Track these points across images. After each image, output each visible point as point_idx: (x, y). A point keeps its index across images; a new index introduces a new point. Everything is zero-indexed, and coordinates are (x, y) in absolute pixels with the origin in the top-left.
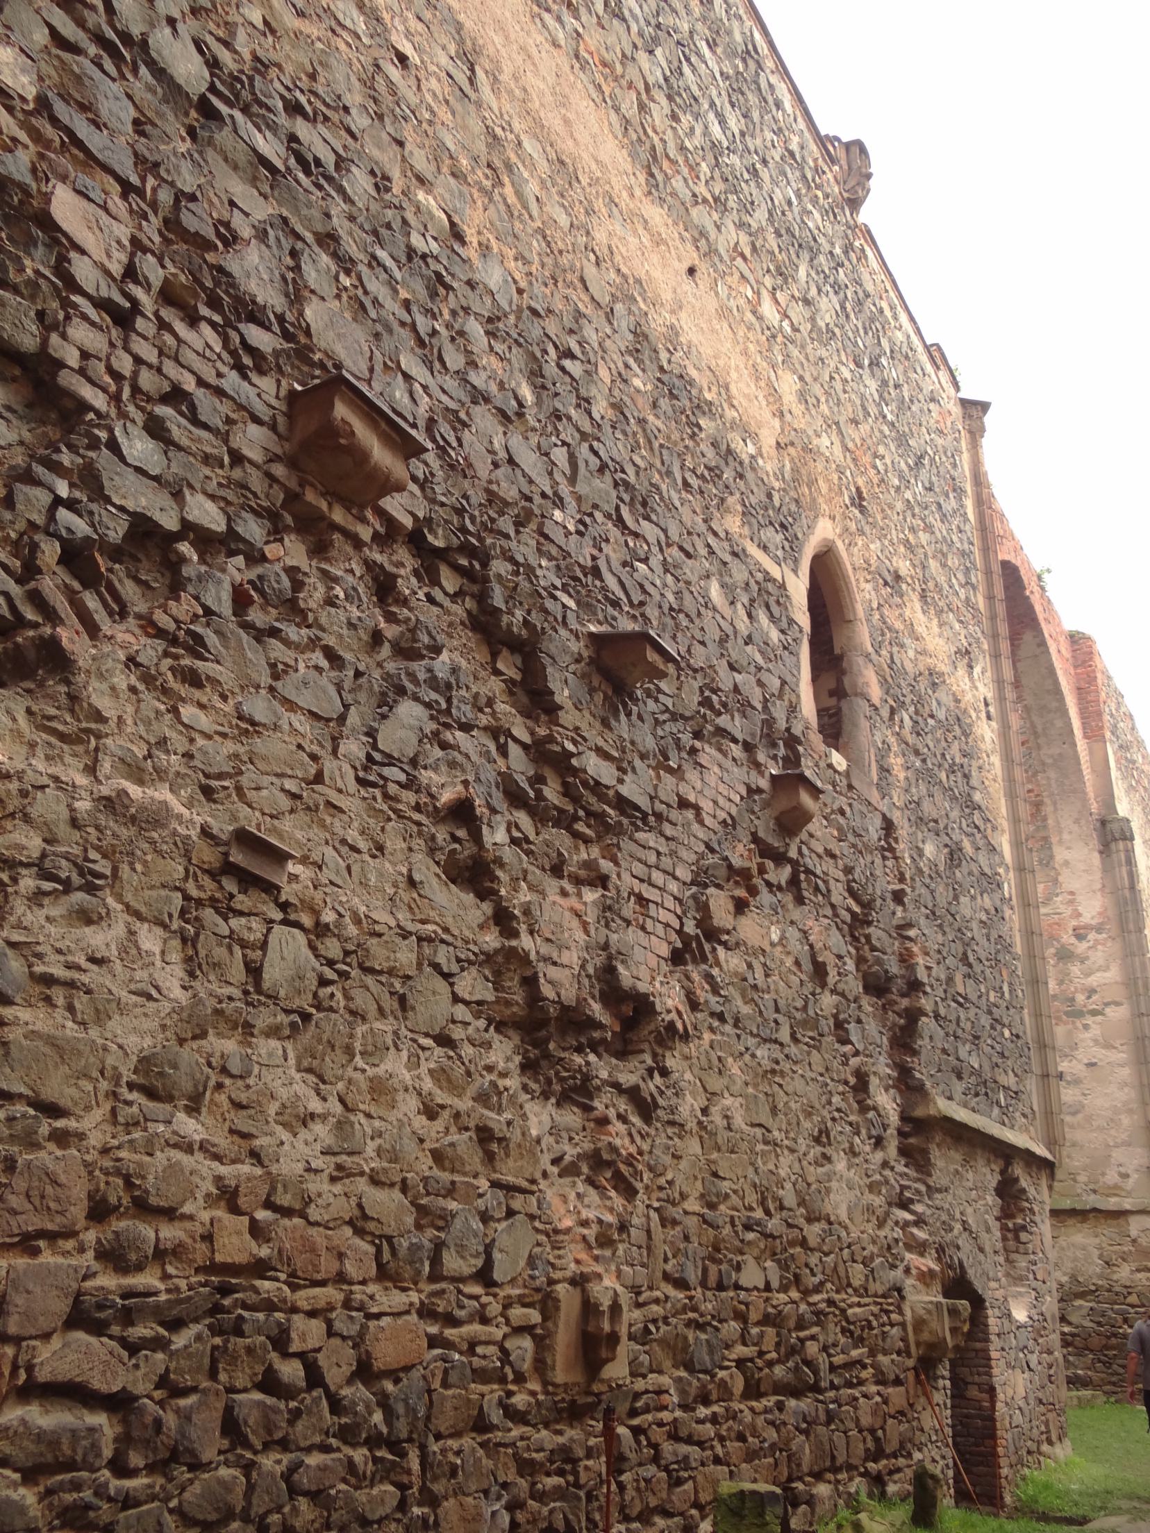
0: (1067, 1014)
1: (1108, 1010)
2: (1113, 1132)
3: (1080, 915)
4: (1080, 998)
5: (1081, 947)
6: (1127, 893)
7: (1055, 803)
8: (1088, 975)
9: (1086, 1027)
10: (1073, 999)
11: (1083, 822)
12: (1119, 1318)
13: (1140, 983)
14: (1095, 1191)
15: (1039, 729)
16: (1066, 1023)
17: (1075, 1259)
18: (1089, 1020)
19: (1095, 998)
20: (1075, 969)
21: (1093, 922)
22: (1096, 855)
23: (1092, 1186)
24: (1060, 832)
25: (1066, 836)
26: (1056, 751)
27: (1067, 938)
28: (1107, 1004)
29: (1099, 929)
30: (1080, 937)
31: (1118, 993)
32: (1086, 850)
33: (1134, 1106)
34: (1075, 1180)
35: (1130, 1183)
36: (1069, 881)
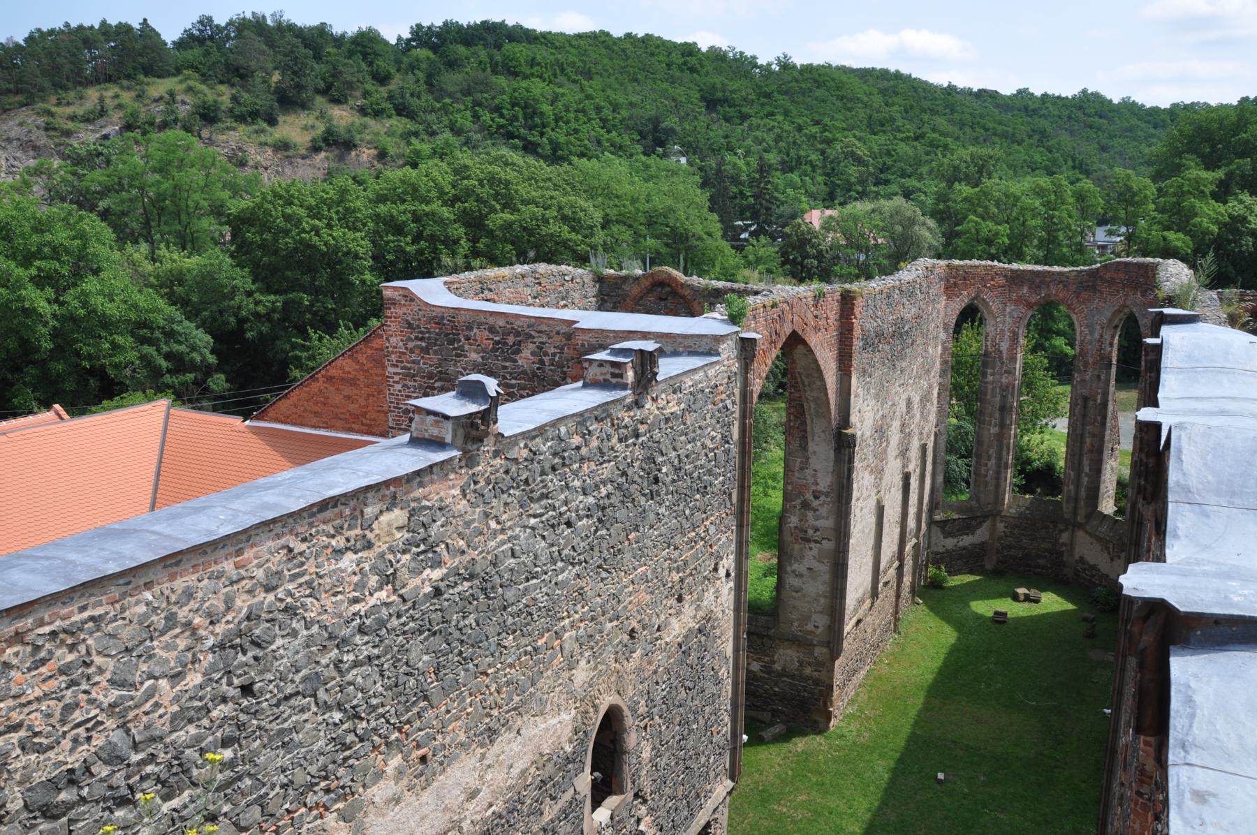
0: (802, 538)
1: (824, 542)
3: (818, 484)
4: (810, 532)
5: (815, 503)
6: (845, 481)
9: (811, 548)
10: (806, 532)
15: (806, 383)
17: (786, 661)
18: (813, 545)
19: (818, 533)
20: (810, 514)
22: (832, 452)
24: (813, 436)
25: (816, 438)
26: (815, 394)
27: (809, 496)
28: (824, 539)
29: (827, 495)
30: (816, 497)
35: (819, 632)
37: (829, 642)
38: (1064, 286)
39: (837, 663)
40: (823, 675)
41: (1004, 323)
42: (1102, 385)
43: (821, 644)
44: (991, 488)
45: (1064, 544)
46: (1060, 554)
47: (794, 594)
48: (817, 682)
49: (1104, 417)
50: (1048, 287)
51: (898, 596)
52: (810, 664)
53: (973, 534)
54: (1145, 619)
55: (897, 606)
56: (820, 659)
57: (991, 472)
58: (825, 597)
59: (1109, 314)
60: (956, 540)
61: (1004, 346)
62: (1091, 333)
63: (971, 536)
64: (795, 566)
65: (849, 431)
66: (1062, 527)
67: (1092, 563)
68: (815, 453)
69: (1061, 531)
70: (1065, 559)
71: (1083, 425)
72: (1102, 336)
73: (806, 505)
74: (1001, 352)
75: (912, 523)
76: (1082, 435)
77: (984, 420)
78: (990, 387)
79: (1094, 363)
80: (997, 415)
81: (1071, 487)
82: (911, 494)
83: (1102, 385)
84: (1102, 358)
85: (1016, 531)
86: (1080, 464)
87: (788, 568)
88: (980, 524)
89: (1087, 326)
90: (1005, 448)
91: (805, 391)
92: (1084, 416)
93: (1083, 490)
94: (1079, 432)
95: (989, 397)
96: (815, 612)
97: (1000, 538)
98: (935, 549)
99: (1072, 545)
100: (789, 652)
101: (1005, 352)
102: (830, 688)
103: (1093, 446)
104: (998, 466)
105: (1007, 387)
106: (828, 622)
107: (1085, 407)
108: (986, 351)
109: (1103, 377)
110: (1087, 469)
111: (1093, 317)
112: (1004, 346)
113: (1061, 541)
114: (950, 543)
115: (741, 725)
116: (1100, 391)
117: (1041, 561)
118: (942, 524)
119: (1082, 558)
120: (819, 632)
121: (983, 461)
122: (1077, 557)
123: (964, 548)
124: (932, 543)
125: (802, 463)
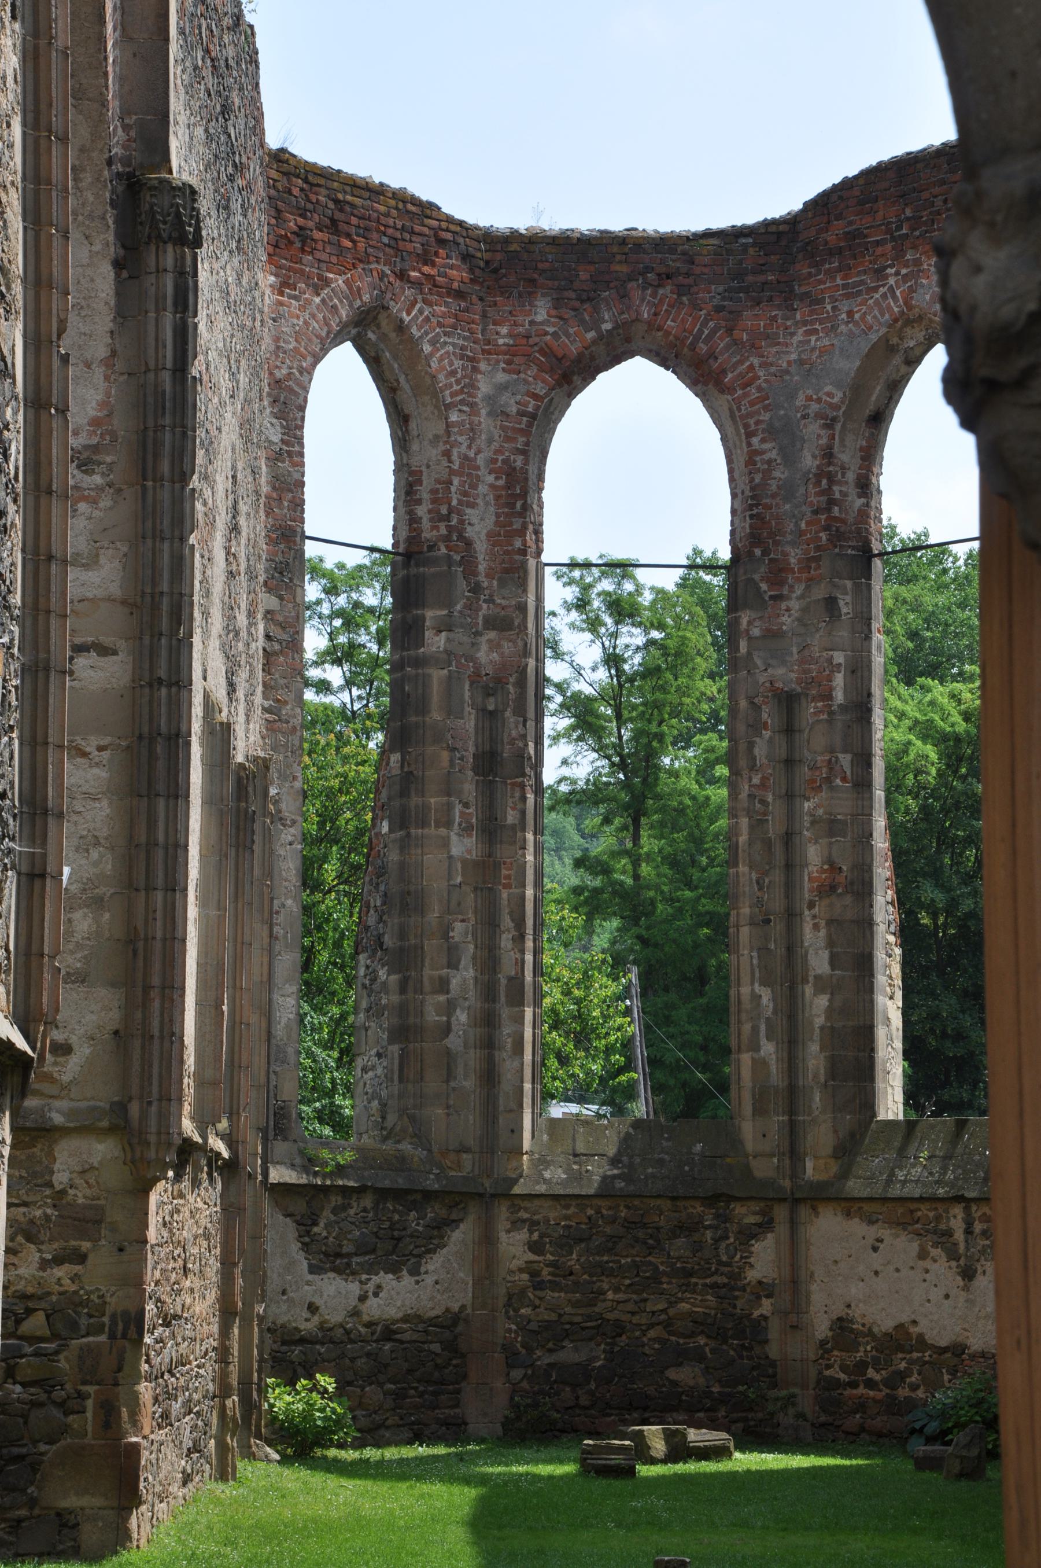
6: (166, 377)
22: (106, 272)
28: (79, 649)
37: (120, 1108)
38: (681, 290)
41: (473, 431)
42: (843, 634)
44: (468, 1082)
45: (764, 1289)
50: (624, 296)
53: (415, 1272)
56: (80, 1196)
57: (462, 1017)
58: (97, 903)
59: (849, 366)
60: (354, 1288)
62: (789, 458)
63: (408, 1280)
66: (746, 1214)
67: (886, 1324)
69: (749, 1235)
70: (773, 1351)
71: (790, 797)
72: (828, 455)
74: (469, 543)
76: (789, 838)
78: (437, 675)
79: (808, 563)
80: (469, 788)
81: (768, 1049)
83: (843, 634)
84: (837, 537)
85: (573, 1260)
86: (792, 948)
88: (441, 1227)
89: (772, 433)
90: (507, 922)
92: (790, 763)
93: (814, 1048)
94: (774, 828)
95: (436, 715)
97: (514, 1299)
101: (481, 547)
103: (834, 868)
104: (488, 992)
106: (113, 1018)
107: (789, 730)
110: (819, 962)
111: (792, 396)
113: (752, 1275)
116: (839, 658)
117: (686, 1375)
119: (842, 1325)
122: (822, 1328)
123: (389, 1333)
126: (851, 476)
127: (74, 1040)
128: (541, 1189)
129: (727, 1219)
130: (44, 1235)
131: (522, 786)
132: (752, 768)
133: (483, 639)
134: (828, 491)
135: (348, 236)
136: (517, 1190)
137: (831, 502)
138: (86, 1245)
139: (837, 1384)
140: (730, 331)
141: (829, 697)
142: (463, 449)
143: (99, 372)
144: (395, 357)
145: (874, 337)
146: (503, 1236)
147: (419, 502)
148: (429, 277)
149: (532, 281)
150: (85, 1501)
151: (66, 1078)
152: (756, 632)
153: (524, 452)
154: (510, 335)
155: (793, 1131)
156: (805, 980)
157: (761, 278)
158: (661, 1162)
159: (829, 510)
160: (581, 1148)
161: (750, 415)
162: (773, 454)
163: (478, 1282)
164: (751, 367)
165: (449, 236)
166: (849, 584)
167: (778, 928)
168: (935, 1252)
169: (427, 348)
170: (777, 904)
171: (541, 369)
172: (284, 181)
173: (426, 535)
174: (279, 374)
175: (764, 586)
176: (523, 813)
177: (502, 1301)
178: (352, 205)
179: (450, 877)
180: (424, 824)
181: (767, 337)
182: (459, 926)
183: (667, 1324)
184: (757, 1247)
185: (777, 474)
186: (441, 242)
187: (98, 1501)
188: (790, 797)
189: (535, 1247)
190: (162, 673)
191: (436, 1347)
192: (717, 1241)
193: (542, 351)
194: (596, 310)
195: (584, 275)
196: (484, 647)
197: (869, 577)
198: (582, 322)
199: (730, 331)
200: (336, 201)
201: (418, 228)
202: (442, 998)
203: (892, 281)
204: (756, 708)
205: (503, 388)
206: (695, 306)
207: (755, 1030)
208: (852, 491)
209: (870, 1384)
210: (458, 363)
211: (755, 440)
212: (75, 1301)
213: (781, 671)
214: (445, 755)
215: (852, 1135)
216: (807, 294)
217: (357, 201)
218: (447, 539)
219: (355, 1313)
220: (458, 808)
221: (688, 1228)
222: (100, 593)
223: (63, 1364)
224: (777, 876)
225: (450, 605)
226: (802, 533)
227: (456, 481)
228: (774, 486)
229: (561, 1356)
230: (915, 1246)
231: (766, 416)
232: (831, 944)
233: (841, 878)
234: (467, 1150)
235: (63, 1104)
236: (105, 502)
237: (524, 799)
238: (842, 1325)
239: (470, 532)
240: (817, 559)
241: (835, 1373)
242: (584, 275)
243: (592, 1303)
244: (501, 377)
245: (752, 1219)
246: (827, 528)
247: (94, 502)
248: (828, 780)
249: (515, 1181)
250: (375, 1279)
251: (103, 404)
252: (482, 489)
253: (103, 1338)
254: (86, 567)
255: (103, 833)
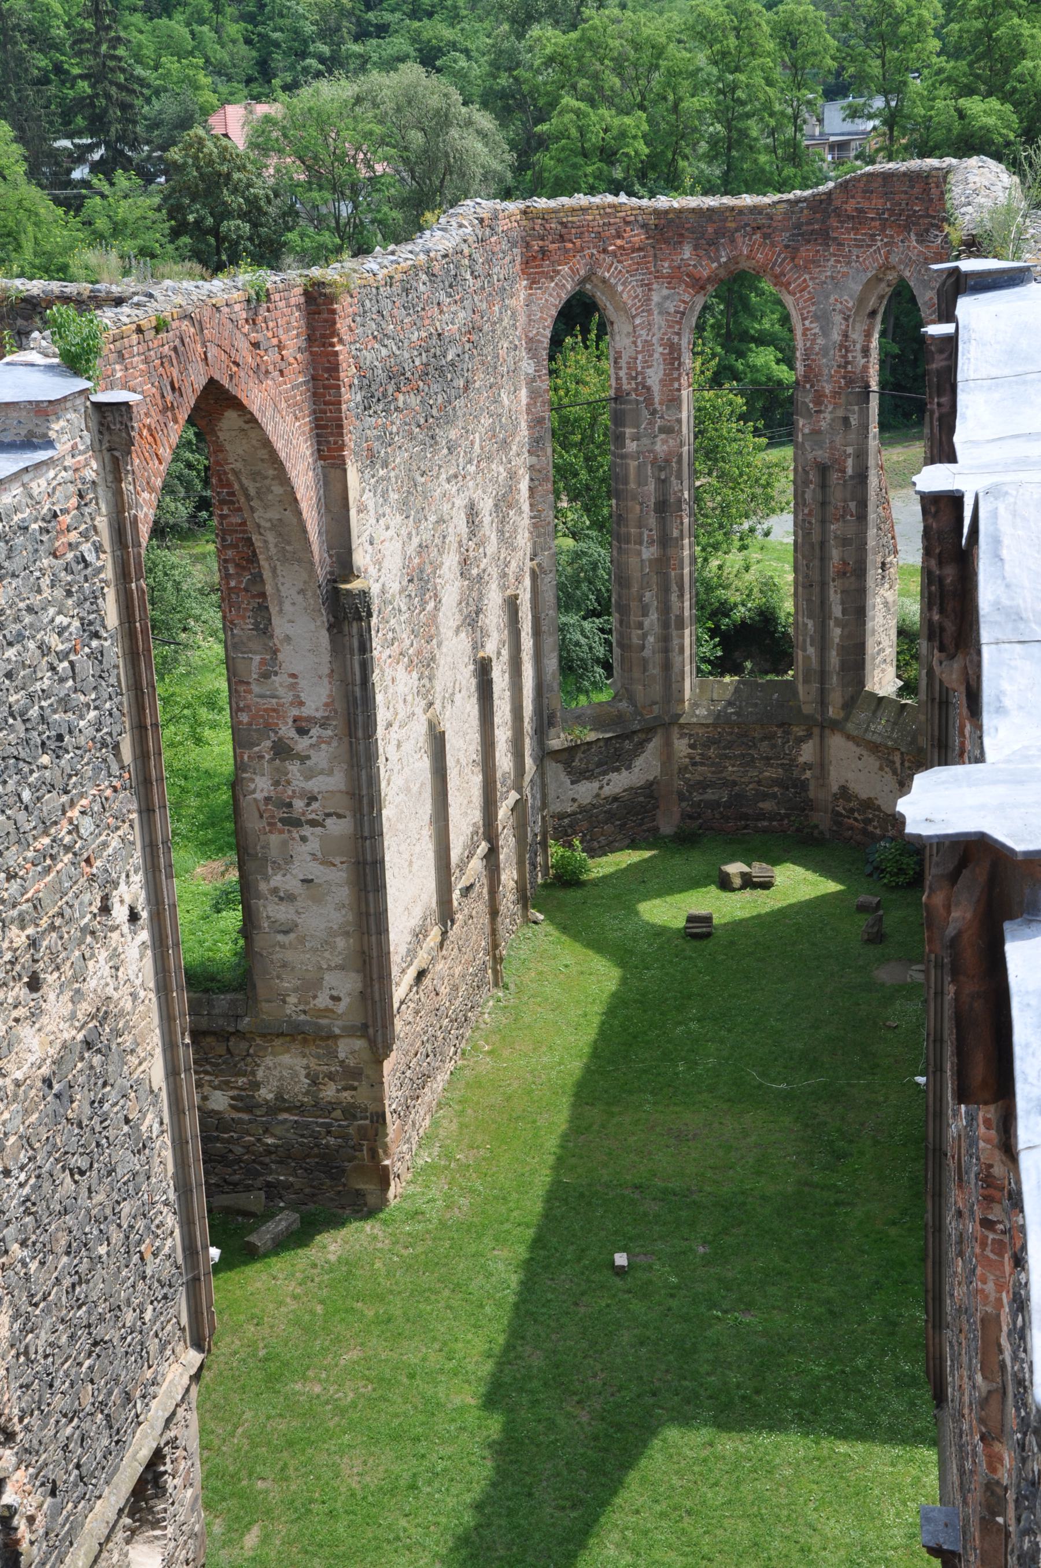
0: (283, 821)
1: (329, 822)
2: (327, 954)
3: (301, 704)
4: (299, 804)
5: (302, 744)
6: (357, 689)
7: (274, 570)
8: (308, 778)
9: (304, 839)
10: (290, 805)
11: (309, 594)
12: (323, 1130)
13: (365, 801)
14: (305, 1012)
15: (252, 492)
16: (281, 832)
18: (307, 831)
19: (315, 805)
20: (294, 768)
21: (318, 715)
23: (301, 1007)
24: (281, 604)
25: (287, 607)
26: (274, 514)
27: (287, 731)
30: (302, 732)
31: (342, 804)
32: (312, 627)
33: (351, 929)
34: (284, 1002)
35: (341, 1007)
36: (291, 659)
37: (365, 1026)
38: (765, 236)
39: (388, 1065)
40: (362, 1096)
42: (852, 436)
43: (351, 1032)
44: (655, 671)
45: (807, 766)
46: (803, 785)
47: (280, 938)
48: (350, 1112)
49: (863, 504)
50: (733, 241)
51: (494, 913)
52: (331, 1077)
53: (629, 768)
54: (953, 877)
55: (494, 932)
57: (651, 639)
58: (347, 934)
59: (857, 288)
60: (596, 785)
61: (654, 377)
62: (825, 333)
63: (625, 773)
64: (277, 880)
65: (355, 585)
66: (799, 731)
67: (864, 795)
68: (288, 639)
69: (800, 740)
70: (811, 794)
71: (823, 522)
72: (846, 336)
73: (282, 751)
74: (649, 389)
75: (504, 761)
76: (823, 544)
77: (629, 534)
78: (633, 464)
79: (835, 394)
80: (652, 521)
81: (811, 651)
82: (497, 702)
83: (852, 436)
84: (850, 382)
86: (824, 602)
87: (263, 887)
88: (641, 746)
89: (816, 318)
90: (674, 588)
91: (252, 510)
92: (824, 504)
93: (834, 653)
94: (816, 538)
95: (632, 486)
96: (330, 969)
97: (683, 770)
98: (556, 807)
99: (822, 766)
100: (286, 1059)
101: (656, 388)
102: (380, 1118)
103: (845, 563)
104: (665, 625)
105: (667, 461)
106: (359, 986)
107: (824, 486)
108: (619, 389)
109: (854, 421)
110: (837, 611)
111: (827, 297)
112: (654, 377)
113: (801, 760)
114: (586, 791)
115: (202, 1228)
117: (767, 806)
118: (567, 756)
119: (844, 789)
120: (341, 1007)
121: (633, 619)
122: (835, 789)
123: (615, 799)
124: (552, 794)
125: (263, 662)
126: (858, 347)
127: (342, 995)
128: (694, 720)
129: (788, 733)
130: (337, 1078)
131: (681, 517)
132: (804, 505)
133: (658, 439)
134: (845, 356)
135: (571, 241)
136: (682, 721)
137: (847, 363)
138: (356, 1084)
139: (841, 815)
140: (793, 259)
141: (844, 472)
142: (644, 337)
143: (326, 680)
144: (603, 294)
145: (869, 275)
146: (676, 741)
147: (620, 368)
148: (621, 247)
149: (681, 235)
150: (367, 1187)
151: (340, 1012)
152: (807, 431)
153: (678, 334)
154: (670, 267)
155: (823, 692)
156: (830, 618)
157: (811, 228)
158: (756, 705)
159: (845, 367)
160: (715, 697)
161: (804, 308)
162: (817, 330)
163: (663, 764)
164: (805, 280)
165: (632, 218)
166: (856, 408)
167: (816, 589)
168: (887, 769)
169: (620, 288)
170: (816, 577)
171: (687, 286)
172: (530, 224)
173: (625, 387)
174: (531, 335)
175: (811, 405)
176: (682, 531)
177: (676, 771)
178: (573, 222)
179: (642, 570)
180: (628, 542)
181: (814, 262)
182: (648, 594)
183: (759, 783)
184: (804, 746)
185: (819, 341)
186: (627, 223)
187: (373, 1187)
188: (823, 522)
189: (692, 746)
190: (366, 834)
191: (641, 799)
192: (784, 744)
193: (688, 275)
194: (717, 250)
195: (710, 230)
196: (659, 443)
197: (868, 403)
198: (710, 258)
199: (793, 259)
200: (562, 223)
201: (612, 221)
202: (640, 632)
203: (879, 244)
204: (806, 473)
205: (666, 298)
206: (773, 245)
207: (804, 641)
208: (859, 355)
209: (856, 819)
210: (639, 290)
211: (807, 322)
212: (353, 1106)
213: (820, 452)
214: (638, 507)
215: (852, 698)
216: (835, 239)
217: (575, 219)
218: (636, 390)
219: (598, 795)
220: (646, 533)
221: (769, 737)
222: (335, 788)
223: (351, 1131)
224: (817, 563)
225: (638, 427)
226: (832, 376)
227: (640, 357)
228: (817, 348)
229: (706, 797)
230: (877, 764)
231: (813, 308)
232: (843, 603)
233: (849, 569)
234: (656, 703)
235: (339, 1023)
236: (335, 744)
237: (682, 523)
238: (844, 789)
239: (649, 382)
240: (839, 393)
241: (840, 809)
242: (710, 230)
243: (721, 772)
244: (665, 292)
245: (801, 733)
246: (844, 378)
247: (329, 743)
248: (843, 516)
249: (680, 716)
250: (607, 777)
251: (330, 696)
252: (656, 356)
253: (367, 1122)
254: (328, 775)
255: (347, 902)
